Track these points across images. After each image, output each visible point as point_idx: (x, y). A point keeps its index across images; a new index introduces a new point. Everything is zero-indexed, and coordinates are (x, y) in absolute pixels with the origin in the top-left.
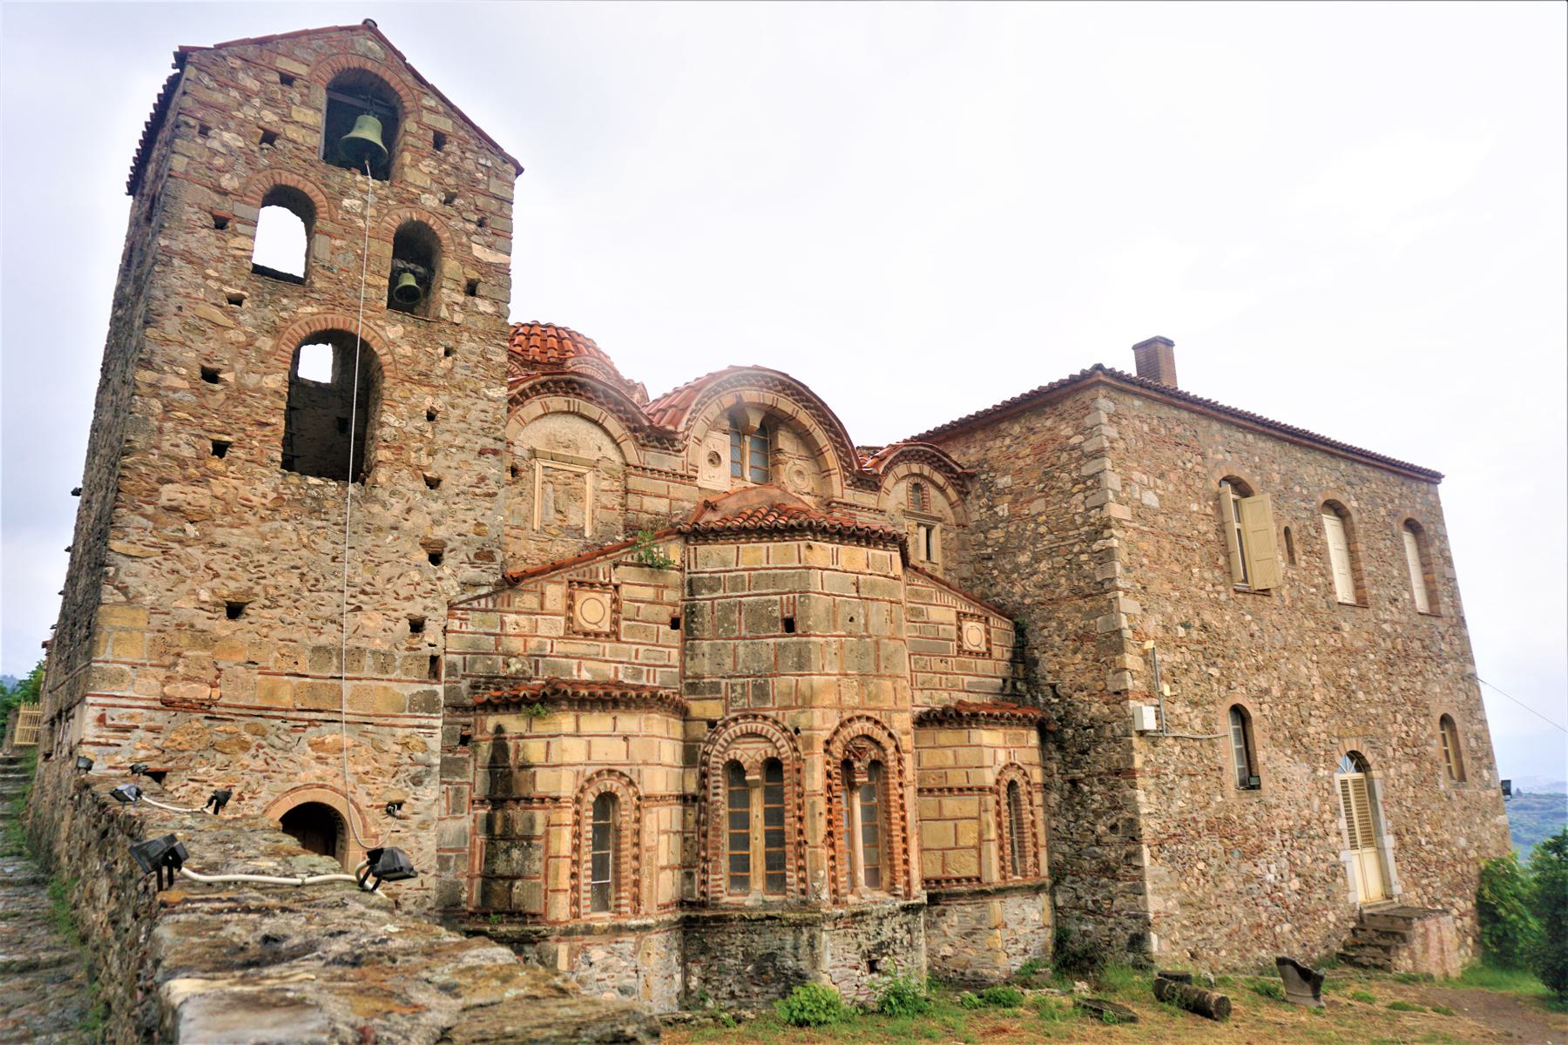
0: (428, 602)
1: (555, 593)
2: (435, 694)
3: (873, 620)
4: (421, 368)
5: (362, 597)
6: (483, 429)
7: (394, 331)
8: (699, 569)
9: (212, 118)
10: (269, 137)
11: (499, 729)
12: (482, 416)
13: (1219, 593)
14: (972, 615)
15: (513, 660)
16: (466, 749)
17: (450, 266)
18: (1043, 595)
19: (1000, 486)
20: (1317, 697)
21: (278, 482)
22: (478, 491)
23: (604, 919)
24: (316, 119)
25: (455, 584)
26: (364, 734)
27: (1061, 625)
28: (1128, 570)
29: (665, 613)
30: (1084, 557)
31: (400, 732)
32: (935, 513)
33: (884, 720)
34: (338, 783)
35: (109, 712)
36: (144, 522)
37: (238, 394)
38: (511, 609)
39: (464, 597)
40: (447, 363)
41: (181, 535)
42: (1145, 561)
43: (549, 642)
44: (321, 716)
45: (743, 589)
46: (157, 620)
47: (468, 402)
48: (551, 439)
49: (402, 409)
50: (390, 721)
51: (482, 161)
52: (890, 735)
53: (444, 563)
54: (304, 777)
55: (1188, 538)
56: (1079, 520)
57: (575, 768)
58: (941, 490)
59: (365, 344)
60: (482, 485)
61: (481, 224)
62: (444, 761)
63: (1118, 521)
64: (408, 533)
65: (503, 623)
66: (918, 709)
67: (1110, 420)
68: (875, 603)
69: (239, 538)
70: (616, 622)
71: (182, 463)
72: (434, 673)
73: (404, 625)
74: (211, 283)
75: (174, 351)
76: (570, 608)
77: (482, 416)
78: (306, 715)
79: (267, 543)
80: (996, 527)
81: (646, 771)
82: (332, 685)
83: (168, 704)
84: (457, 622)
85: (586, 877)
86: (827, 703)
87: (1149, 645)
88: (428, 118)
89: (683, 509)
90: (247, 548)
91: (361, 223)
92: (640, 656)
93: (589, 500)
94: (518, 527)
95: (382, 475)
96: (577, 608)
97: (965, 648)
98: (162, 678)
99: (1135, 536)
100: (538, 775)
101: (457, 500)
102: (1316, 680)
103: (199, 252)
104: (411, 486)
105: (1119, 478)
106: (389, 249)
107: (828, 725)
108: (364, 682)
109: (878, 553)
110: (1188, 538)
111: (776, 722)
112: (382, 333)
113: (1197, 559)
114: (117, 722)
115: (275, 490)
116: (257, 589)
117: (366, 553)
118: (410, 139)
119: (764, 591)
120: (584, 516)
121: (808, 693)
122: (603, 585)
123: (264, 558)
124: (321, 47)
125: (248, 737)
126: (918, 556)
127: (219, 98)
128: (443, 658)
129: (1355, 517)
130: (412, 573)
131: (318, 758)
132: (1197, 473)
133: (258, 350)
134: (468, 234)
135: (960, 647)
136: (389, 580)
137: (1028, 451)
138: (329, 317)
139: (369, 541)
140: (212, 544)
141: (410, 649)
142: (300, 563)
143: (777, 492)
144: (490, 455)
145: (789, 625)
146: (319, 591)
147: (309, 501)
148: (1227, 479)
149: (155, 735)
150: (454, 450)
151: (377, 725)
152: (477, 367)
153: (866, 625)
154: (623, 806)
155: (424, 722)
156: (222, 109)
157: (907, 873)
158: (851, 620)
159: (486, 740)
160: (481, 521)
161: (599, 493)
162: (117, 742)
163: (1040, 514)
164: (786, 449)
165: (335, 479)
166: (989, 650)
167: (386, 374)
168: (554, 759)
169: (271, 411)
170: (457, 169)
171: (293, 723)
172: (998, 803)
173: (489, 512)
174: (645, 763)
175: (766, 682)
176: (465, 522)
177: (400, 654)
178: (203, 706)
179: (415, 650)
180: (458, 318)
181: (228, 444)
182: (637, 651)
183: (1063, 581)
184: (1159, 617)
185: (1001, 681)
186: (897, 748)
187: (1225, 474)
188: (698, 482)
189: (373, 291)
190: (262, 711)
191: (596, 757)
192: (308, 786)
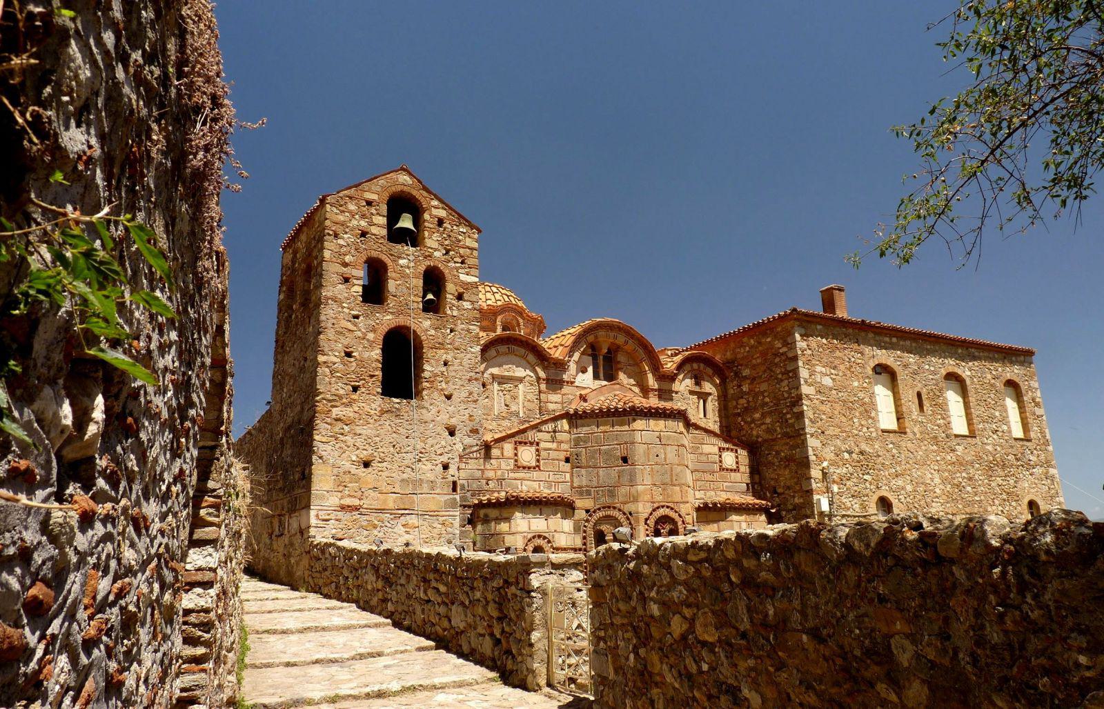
0: (450, 455)
1: (508, 447)
2: (455, 499)
3: (669, 456)
4: (440, 340)
5: (420, 455)
7: (427, 323)
9: (339, 229)
10: (364, 234)
11: (486, 515)
14: (728, 449)
15: (490, 482)
17: (450, 287)
18: (766, 436)
19: (744, 374)
20: (937, 490)
24: (382, 221)
27: (778, 453)
29: (562, 456)
31: (441, 519)
33: (675, 508)
35: (320, 513)
36: (326, 425)
37: (361, 362)
44: (407, 512)
51: (461, 230)
52: (680, 516)
59: (414, 331)
61: (463, 262)
62: (462, 532)
69: (366, 431)
70: (538, 461)
71: (341, 397)
72: (454, 490)
74: (345, 310)
76: (516, 455)
78: (400, 512)
81: (557, 535)
83: (343, 508)
87: (825, 464)
88: (435, 212)
91: (408, 271)
93: (521, 398)
96: (519, 454)
98: (339, 496)
102: (937, 480)
103: (339, 296)
106: (421, 283)
111: (620, 510)
115: (380, 406)
116: (376, 454)
118: (426, 224)
120: (519, 407)
121: (636, 494)
125: (376, 522)
126: (695, 416)
127: (341, 218)
129: (968, 382)
133: (368, 340)
134: (457, 269)
136: (432, 446)
141: (443, 478)
142: (392, 440)
145: (625, 460)
153: (665, 458)
155: (451, 513)
156: (343, 224)
164: (622, 361)
168: (513, 530)
169: (376, 369)
170: (450, 236)
177: (439, 480)
178: (357, 509)
180: (455, 313)
181: (359, 386)
183: (778, 429)
186: (683, 522)
188: (576, 384)
190: (381, 511)
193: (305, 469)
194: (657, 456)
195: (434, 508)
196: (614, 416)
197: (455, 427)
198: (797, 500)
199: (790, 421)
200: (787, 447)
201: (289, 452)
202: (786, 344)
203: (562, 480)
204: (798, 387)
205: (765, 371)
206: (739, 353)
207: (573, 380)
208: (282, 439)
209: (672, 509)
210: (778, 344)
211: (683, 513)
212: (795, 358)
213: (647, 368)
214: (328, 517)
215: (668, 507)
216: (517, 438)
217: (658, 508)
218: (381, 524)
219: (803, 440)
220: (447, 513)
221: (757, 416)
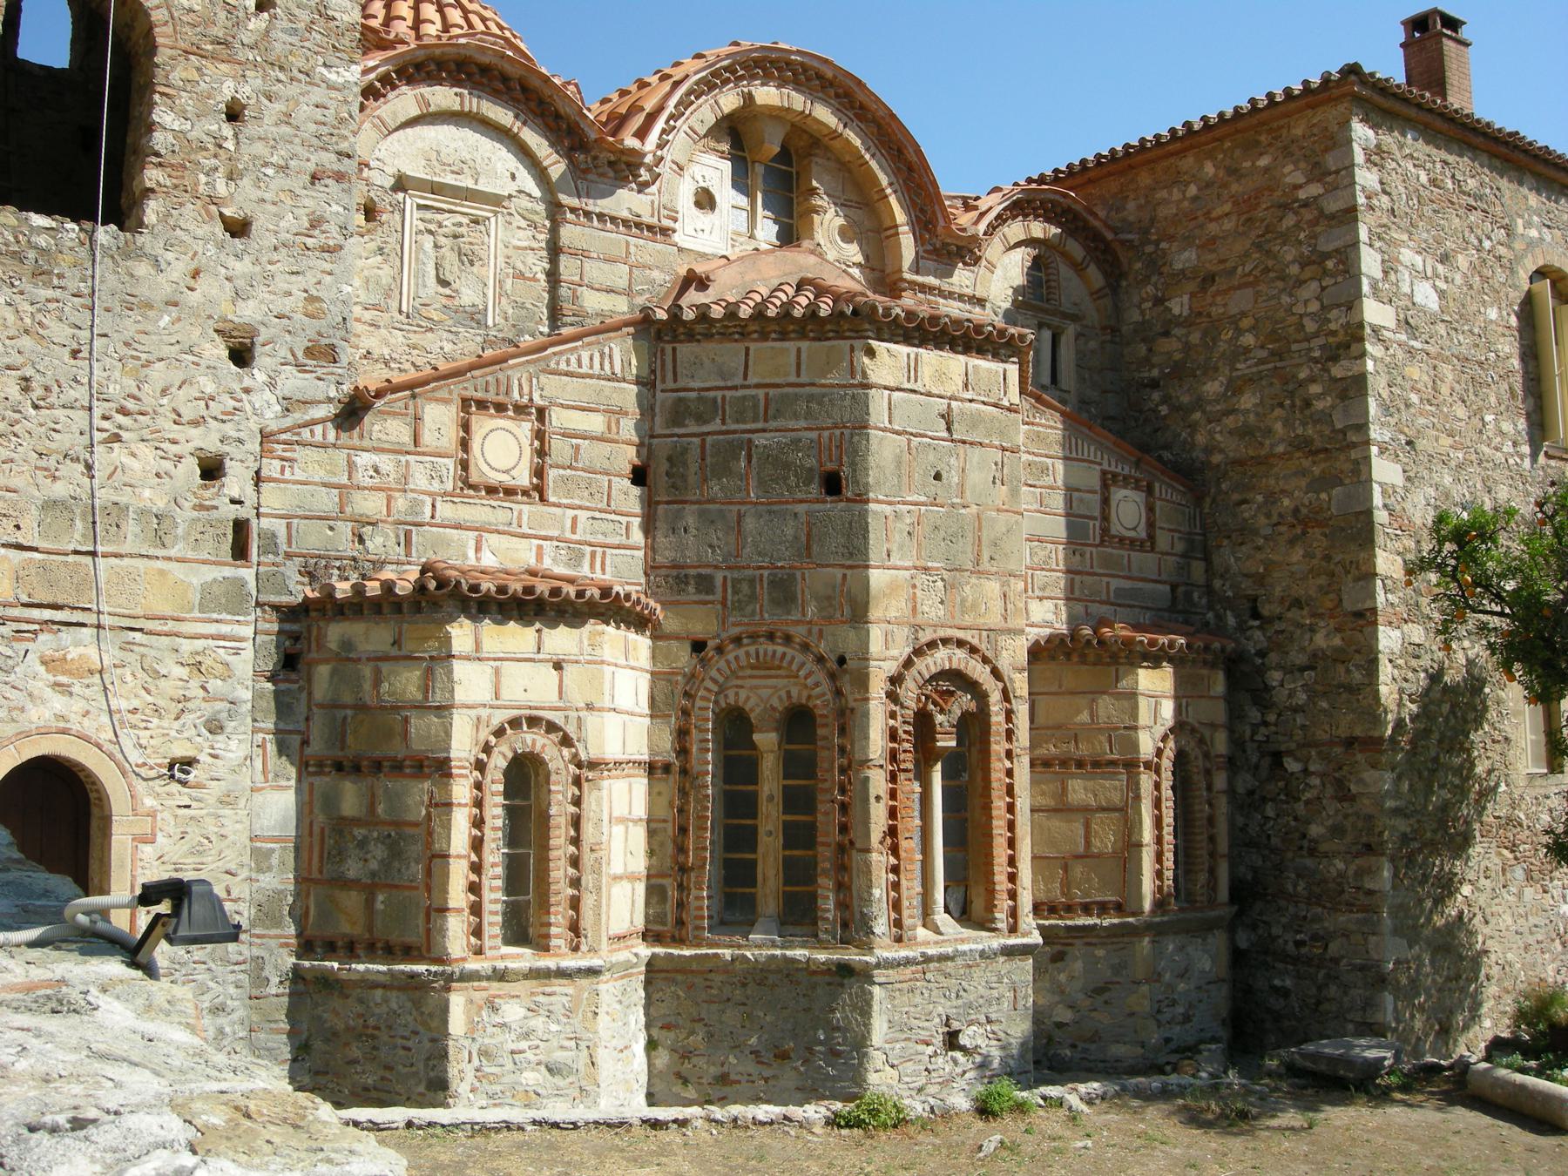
0: (229, 429)
1: (440, 418)
2: (242, 583)
5: (120, 418)
8: (680, 384)
11: (347, 645)
12: (318, 114)
13: (1522, 457)
14: (1125, 478)
16: (294, 676)
19: (1178, 266)
22: (310, 242)
23: (521, 958)
25: (273, 400)
26: (127, 646)
27: (1271, 498)
30: (1315, 389)
31: (187, 646)
32: (1066, 306)
34: (88, 726)
38: (366, 443)
39: (288, 422)
40: (258, 23)
42: (1414, 398)
43: (429, 501)
45: (755, 420)
47: (294, 90)
48: (435, 157)
49: (184, 99)
50: (170, 626)
52: (996, 673)
54: (37, 715)
55: (1481, 364)
56: (1310, 326)
57: (473, 713)
58: (1078, 268)
60: (316, 232)
63: (1376, 330)
64: (195, 312)
65: (351, 466)
66: (1035, 630)
67: (1368, 160)
68: (977, 450)
70: (539, 473)
73: (191, 467)
76: (465, 445)
77: (318, 114)
78: (36, 614)
80: (1166, 334)
81: (591, 719)
82: (76, 564)
84: (277, 464)
85: (492, 889)
86: (892, 614)
89: (652, 282)
92: (580, 526)
94: (376, 307)
95: (152, 211)
97: (1113, 532)
99: (1400, 354)
101: (275, 257)
104: (200, 232)
105: (1379, 257)
107: (894, 652)
108: (127, 561)
109: (986, 366)
110: (1481, 364)
113: (1493, 400)
117: (127, 344)
122: (520, 410)
128: (254, 522)
130: (202, 380)
132: (1499, 258)
135: (1105, 531)
136: (164, 392)
137: (1227, 207)
139: (130, 325)
141: (201, 507)
142: (19, 360)
143: (812, 259)
144: (330, 182)
146: (51, 407)
147: (32, 255)
148: (1540, 273)
150: (270, 171)
151: (150, 633)
152: (309, 30)
154: (553, 777)
155: (225, 629)
157: (1013, 895)
158: (938, 477)
159: (326, 661)
160: (315, 293)
161: (510, 252)
165: (75, 220)
166: (1151, 537)
167: (159, 40)
171: (15, 626)
172: (1157, 786)
173: (328, 278)
174: (590, 707)
176: (290, 294)
177: (185, 514)
179: (208, 508)
182: (575, 519)
184: (1431, 492)
185: (1168, 588)
187: (1541, 263)
188: (676, 238)
191: (506, 695)
192: (44, 732)
195: (168, 612)
196: (803, 336)
197: (253, 333)
198: (1320, 640)
199: (1319, 405)
200: (1303, 483)
202: (1318, 173)
203: (616, 540)
204: (1352, 302)
209: (973, 650)
210: (1293, 175)
211: (1004, 664)
212: (1349, 215)
213: (900, 216)
215: (960, 643)
216: (469, 387)
217: (932, 645)
219: (1356, 462)
220: (212, 629)
221: (1212, 388)
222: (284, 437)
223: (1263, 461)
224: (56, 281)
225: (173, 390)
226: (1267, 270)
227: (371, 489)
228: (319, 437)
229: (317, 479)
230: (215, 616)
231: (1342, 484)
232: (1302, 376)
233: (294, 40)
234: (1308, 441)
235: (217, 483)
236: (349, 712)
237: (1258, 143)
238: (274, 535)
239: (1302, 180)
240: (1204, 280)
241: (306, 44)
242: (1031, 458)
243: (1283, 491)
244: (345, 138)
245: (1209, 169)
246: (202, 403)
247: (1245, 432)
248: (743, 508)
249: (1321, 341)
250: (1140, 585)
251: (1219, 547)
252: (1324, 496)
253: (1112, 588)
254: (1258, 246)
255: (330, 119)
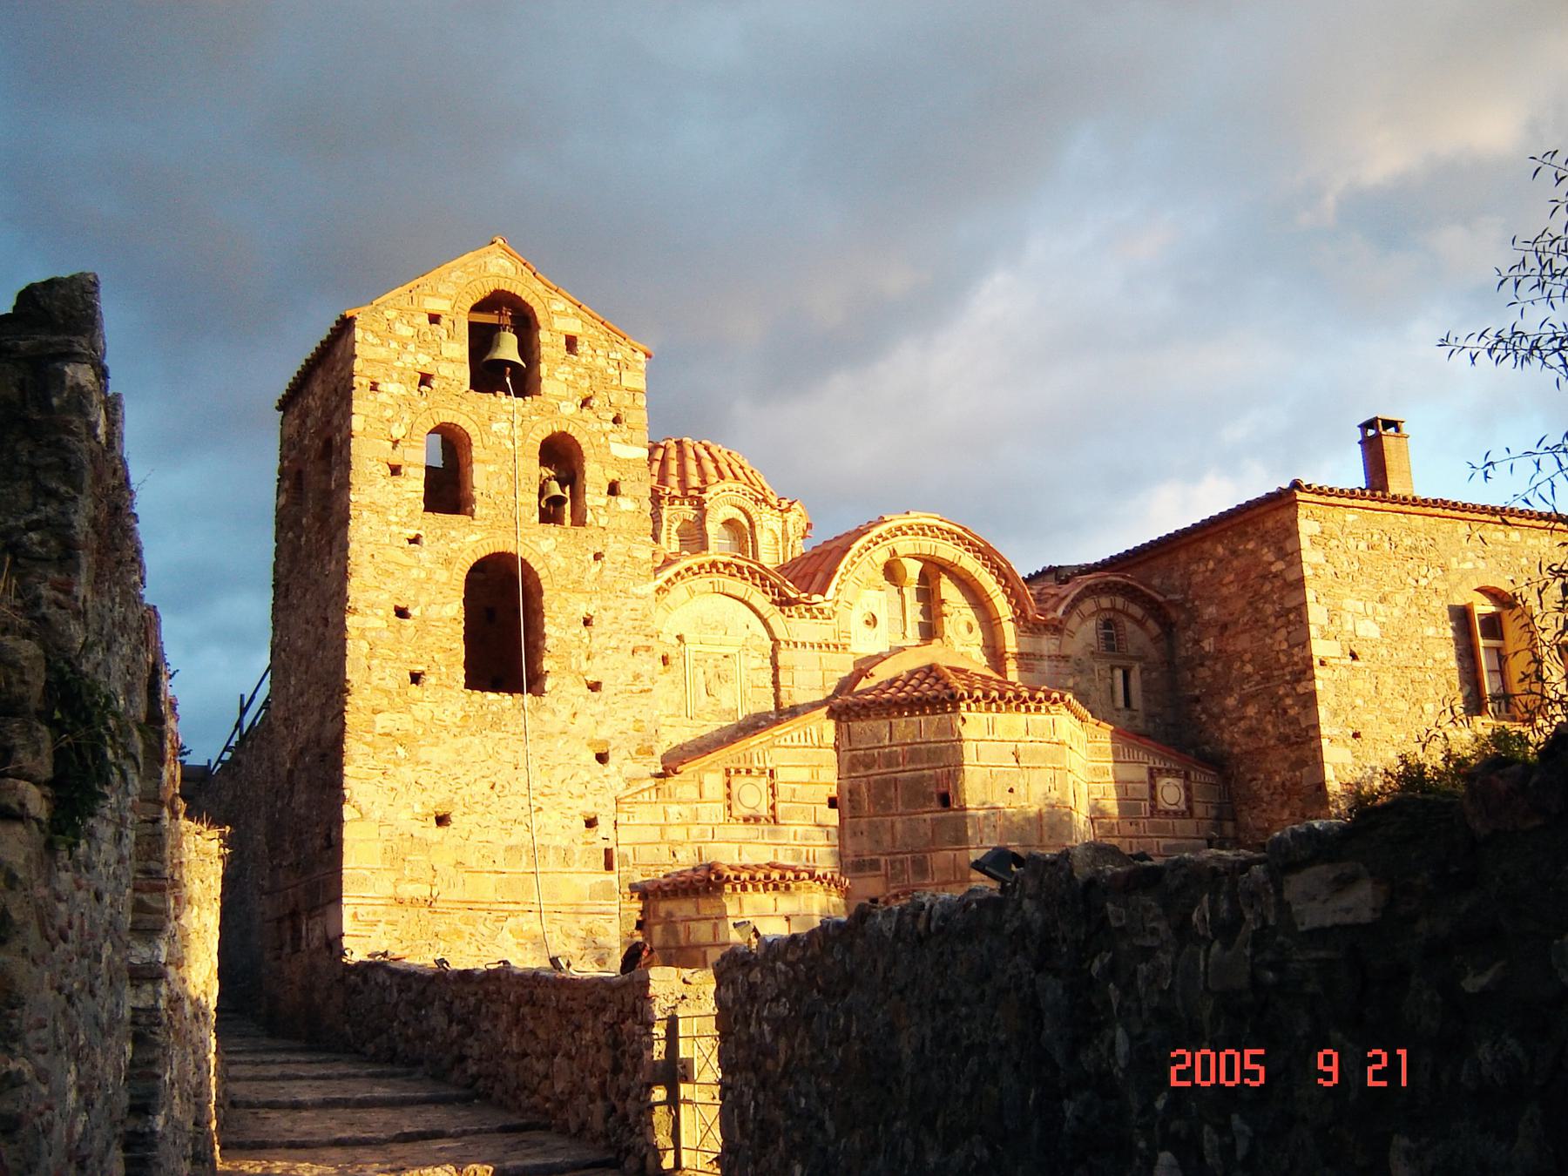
0: (600, 800)
2: (611, 883)
5: (541, 798)
6: (634, 628)
7: (547, 545)
8: (853, 746)
11: (670, 914)
21: (464, 701)
22: (634, 688)
24: (460, 349)
27: (1269, 777)
28: (1335, 714)
35: (360, 910)
39: (629, 792)
41: (394, 756)
45: (898, 765)
46: (385, 831)
47: (618, 603)
53: (610, 761)
56: (1283, 659)
60: (637, 683)
65: (665, 812)
68: (1037, 772)
69: (436, 756)
71: (388, 693)
72: (609, 866)
75: (372, 595)
78: (505, 906)
79: (460, 758)
90: (446, 763)
95: (549, 684)
97: (1160, 807)
100: (708, 952)
103: (381, 502)
108: (550, 876)
112: (537, 549)
114: (366, 918)
115: (463, 709)
116: (457, 798)
119: (919, 766)
123: (459, 770)
124: (458, 278)
125: (463, 927)
128: (615, 850)
130: (582, 773)
131: (518, 944)
135: (1153, 807)
137: (1232, 577)
138: (490, 541)
139: (543, 746)
140: (418, 763)
141: (587, 843)
142: (489, 772)
146: (506, 796)
149: (395, 928)
155: (603, 909)
159: (659, 924)
160: (638, 717)
162: (369, 934)
163: (1245, 651)
166: (1190, 808)
173: (646, 708)
175: (925, 857)
177: (578, 848)
189: (527, 509)
193: (330, 830)
194: (1011, 791)
197: (607, 743)
200: (1286, 766)
201: (304, 797)
204: (1305, 642)
205: (1244, 612)
206: (1195, 572)
207: (844, 641)
208: (291, 772)
214: (371, 917)
218: (470, 929)
219: (1315, 750)
222: (627, 800)
223: (1263, 752)
224: (503, 729)
225: (568, 781)
226: (1257, 621)
227: (678, 825)
228: (647, 799)
229: (648, 822)
230: (598, 902)
231: (1308, 765)
232: (1281, 693)
233: (616, 574)
234: (1287, 737)
235: (594, 829)
236: (674, 951)
237: (1246, 533)
238: (626, 856)
239: (1273, 559)
240: (1222, 627)
241: (623, 575)
242: (1095, 764)
243: (1275, 771)
244: (649, 626)
245: (1220, 550)
246: (583, 786)
247: (1250, 732)
248: (894, 818)
249: (1290, 669)
250: (1183, 841)
251: (1241, 810)
252: (1298, 773)
253: (1161, 844)
254: (1250, 604)
255: (639, 617)
